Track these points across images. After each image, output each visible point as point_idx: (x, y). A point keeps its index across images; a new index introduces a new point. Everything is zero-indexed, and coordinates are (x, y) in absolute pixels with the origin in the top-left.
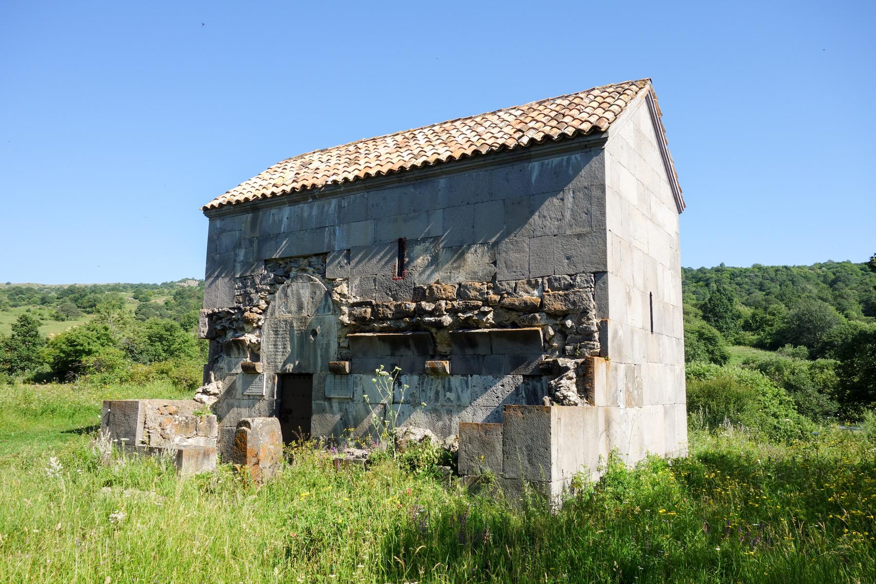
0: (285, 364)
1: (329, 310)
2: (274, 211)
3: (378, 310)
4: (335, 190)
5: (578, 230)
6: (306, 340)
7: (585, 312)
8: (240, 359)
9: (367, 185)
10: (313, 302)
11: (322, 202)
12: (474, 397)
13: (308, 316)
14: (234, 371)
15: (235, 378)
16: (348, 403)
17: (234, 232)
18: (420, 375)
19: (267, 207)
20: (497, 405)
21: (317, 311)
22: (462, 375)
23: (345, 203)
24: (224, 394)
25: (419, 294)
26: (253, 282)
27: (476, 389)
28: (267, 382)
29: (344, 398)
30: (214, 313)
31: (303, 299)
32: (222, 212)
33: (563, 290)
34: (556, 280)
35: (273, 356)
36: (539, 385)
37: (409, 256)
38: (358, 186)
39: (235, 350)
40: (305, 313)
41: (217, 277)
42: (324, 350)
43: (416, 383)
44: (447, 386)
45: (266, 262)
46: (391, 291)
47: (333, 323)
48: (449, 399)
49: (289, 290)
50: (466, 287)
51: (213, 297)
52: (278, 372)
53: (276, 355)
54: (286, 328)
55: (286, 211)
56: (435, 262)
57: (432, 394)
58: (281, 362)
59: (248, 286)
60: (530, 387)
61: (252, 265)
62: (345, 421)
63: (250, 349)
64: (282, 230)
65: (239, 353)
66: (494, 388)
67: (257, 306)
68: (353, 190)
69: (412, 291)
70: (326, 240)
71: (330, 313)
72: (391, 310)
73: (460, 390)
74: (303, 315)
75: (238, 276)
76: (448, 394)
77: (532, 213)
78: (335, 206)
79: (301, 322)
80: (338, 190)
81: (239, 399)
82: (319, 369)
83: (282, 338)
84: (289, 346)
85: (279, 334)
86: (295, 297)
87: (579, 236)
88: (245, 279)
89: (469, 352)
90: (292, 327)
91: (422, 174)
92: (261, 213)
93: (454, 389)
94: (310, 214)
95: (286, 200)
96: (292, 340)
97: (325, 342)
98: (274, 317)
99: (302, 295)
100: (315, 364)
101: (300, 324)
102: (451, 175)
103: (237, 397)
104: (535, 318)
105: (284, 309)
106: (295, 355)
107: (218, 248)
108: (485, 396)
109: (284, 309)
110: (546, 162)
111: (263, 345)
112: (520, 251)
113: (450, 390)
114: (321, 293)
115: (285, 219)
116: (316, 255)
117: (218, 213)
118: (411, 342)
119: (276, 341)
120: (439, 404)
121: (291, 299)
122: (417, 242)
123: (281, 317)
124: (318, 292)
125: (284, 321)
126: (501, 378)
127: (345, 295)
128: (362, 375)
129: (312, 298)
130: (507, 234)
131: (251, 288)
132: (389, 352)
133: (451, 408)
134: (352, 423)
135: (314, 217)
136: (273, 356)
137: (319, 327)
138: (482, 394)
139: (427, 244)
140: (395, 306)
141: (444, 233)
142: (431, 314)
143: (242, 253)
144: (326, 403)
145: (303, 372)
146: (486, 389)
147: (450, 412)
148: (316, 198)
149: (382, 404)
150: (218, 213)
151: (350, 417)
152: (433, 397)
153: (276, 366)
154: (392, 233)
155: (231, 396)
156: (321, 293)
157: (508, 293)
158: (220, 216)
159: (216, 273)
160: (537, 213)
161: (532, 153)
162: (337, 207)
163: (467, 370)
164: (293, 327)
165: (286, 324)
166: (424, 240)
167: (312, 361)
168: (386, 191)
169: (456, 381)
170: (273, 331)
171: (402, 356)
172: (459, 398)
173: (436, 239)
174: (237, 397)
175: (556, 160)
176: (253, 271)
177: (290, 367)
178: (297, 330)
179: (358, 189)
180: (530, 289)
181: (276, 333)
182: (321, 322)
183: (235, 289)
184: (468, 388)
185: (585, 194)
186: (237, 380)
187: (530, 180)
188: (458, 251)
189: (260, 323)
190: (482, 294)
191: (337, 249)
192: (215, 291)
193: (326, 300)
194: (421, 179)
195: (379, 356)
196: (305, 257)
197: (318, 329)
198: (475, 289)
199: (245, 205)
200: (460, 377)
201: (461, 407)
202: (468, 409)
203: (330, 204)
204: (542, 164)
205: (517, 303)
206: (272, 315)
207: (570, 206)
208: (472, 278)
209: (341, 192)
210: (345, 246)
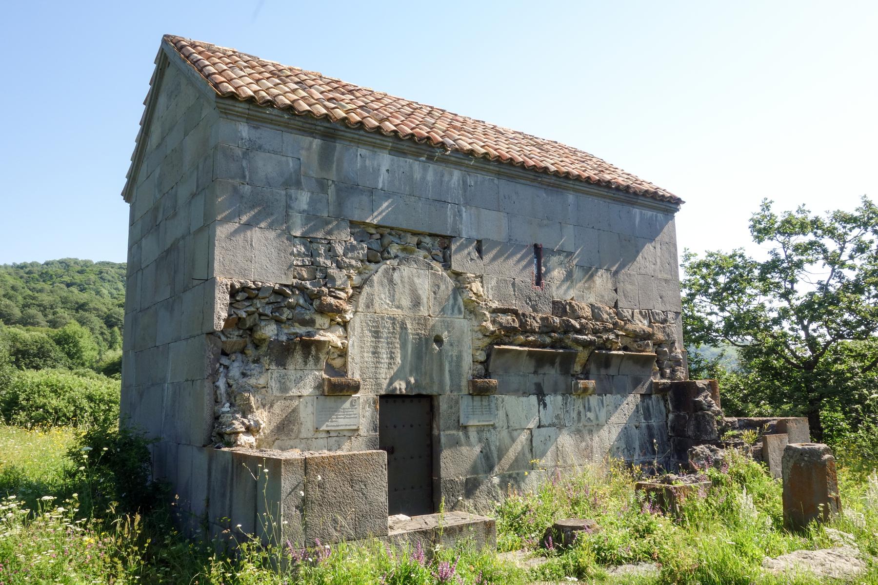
0: (391, 383)
1: (460, 312)
2: (362, 151)
3: (526, 321)
4: (463, 161)
5: (665, 276)
6: (427, 349)
7: (673, 343)
8: (306, 372)
9: (502, 170)
10: (435, 298)
11: (441, 168)
12: (609, 416)
13: (429, 316)
14: (294, 392)
15: (296, 403)
16: (489, 430)
17: (284, 159)
18: (563, 395)
19: (351, 141)
20: (625, 422)
21: (443, 310)
22: (599, 395)
23: (471, 181)
24: (272, 431)
25: (559, 308)
26: (330, 249)
27: (610, 408)
29: (484, 425)
30: (244, 288)
31: (420, 292)
32: (259, 114)
33: (661, 323)
34: (657, 314)
36: (650, 402)
37: (545, 266)
38: (491, 167)
39: (298, 357)
40: (424, 311)
41: (248, 225)
42: (454, 364)
43: (561, 403)
44: (587, 405)
45: (353, 224)
46: (530, 300)
47: (466, 330)
48: (589, 419)
49: (396, 276)
50: (599, 309)
51: (239, 259)
52: (383, 392)
53: (377, 367)
54: (394, 329)
55: (385, 160)
56: (569, 276)
57: (574, 415)
58: (385, 379)
59: (319, 255)
60: (645, 404)
61: (327, 223)
62: (487, 454)
64: (380, 186)
65: (306, 363)
66: (622, 406)
67: (342, 290)
68: (482, 169)
69: (551, 305)
70: (450, 220)
71: (462, 316)
72: (537, 322)
73: (597, 409)
74: (420, 314)
75: (298, 233)
76: (589, 414)
77: (638, 252)
78: (458, 181)
79: (418, 324)
80: (466, 162)
81: (308, 439)
82: (448, 388)
83: (388, 343)
84: (399, 355)
85: (381, 337)
86: (407, 286)
87: (666, 281)
88: (311, 242)
89: (603, 372)
90: (403, 327)
91: (558, 183)
92: (339, 146)
93: (593, 408)
94: (424, 178)
95: (390, 144)
96: (403, 346)
97: (455, 353)
98: (371, 310)
99: (419, 286)
102: (578, 194)
103: (303, 435)
104: (648, 345)
105: (388, 302)
106: (407, 369)
107: (247, 173)
108: (616, 414)
109: (388, 302)
110: (643, 211)
111: (353, 352)
112: (632, 283)
113: (590, 410)
114: (447, 288)
116: (430, 235)
117: (251, 112)
118: (558, 360)
119: (376, 347)
120: (581, 424)
121: (399, 288)
122: (553, 253)
123: (384, 312)
124: (443, 287)
125: (390, 318)
126: (626, 397)
127: (481, 296)
128: (503, 396)
129: (435, 293)
130: (622, 266)
131: (326, 258)
132: (532, 369)
133: (592, 428)
134: (495, 455)
135: (430, 184)
137: (446, 333)
138: (614, 412)
139: (562, 258)
140: (541, 319)
141: (576, 250)
142: (579, 332)
143: (303, 200)
144: (461, 433)
145: (424, 393)
146: (616, 408)
147: (591, 432)
148: (432, 160)
149: (529, 429)
150: (251, 112)
151: (493, 448)
152: (576, 419)
153: (378, 385)
154: (528, 235)
155: (288, 435)
156: (447, 288)
157: (629, 320)
158: (247, 119)
159: (245, 219)
160: (641, 254)
161: (639, 201)
162: (461, 182)
163: (602, 391)
164: (406, 328)
165: (394, 323)
166: (560, 252)
167: (436, 378)
168: (518, 185)
169: (594, 400)
170: (371, 331)
171: (544, 374)
172: (597, 418)
173: (570, 254)
174: (303, 435)
175: (649, 213)
176: (330, 233)
177: (400, 386)
178: (413, 334)
179: (488, 171)
180: (642, 319)
181: (376, 334)
182: (449, 327)
183: (292, 254)
184: (603, 406)
185: (667, 249)
186: (302, 407)
187: (634, 224)
188: (589, 272)
190: (611, 318)
191: (464, 235)
192: (244, 248)
193: (455, 299)
194: (552, 186)
195: (521, 373)
196: (414, 234)
197: (445, 336)
198: (606, 312)
199: (315, 122)
200: (596, 396)
201: (599, 426)
202: (606, 428)
203: (451, 175)
204: (641, 213)
205: (638, 330)
206: (368, 307)
207: (659, 254)
208: (600, 301)
209: (468, 166)
210: (474, 235)
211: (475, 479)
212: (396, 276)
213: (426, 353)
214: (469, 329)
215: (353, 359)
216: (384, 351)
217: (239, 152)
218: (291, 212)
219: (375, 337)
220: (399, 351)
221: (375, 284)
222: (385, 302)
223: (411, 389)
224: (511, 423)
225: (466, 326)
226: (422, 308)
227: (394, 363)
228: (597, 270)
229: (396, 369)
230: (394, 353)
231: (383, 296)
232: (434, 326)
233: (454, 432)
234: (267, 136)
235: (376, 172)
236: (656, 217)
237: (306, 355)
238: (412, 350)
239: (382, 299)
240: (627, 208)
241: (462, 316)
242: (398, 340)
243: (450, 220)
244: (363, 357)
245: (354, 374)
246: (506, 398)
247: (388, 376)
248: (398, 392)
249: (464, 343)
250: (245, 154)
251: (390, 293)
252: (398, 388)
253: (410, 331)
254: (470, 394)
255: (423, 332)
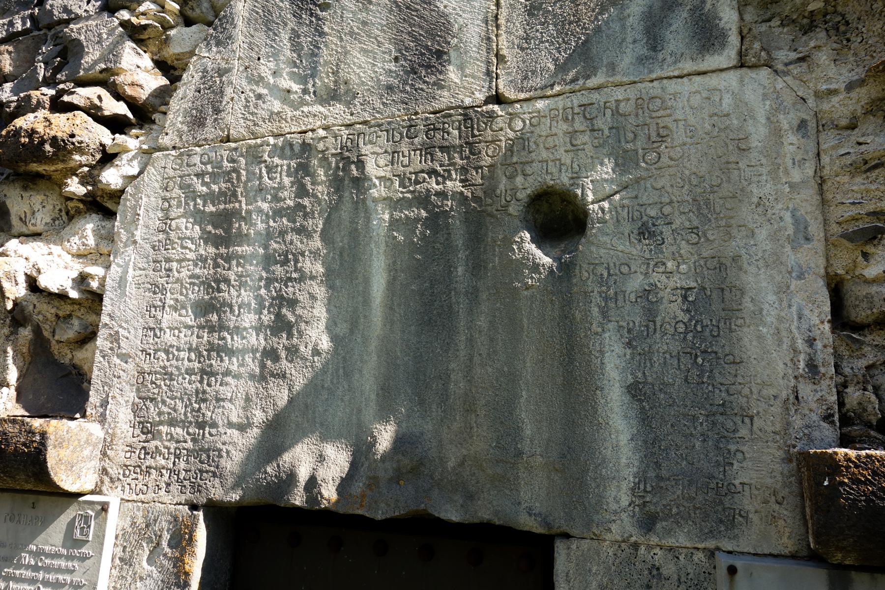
6: (477, 267)
13: (498, 99)
28: (126, 561)
35: (189, 385)
47: (758, 133)
52: (217, 492)
53: (207, 373)
54: (302, 191)
58: (242, 428)
63: (26, 333)
74: (445, 99)
79: (428, 150)
83: (268, 261)
84: (320, 312)
98: (210, 132)
101: (418, 162)
105: (286, 83)
109: (286, 83)
119: (215, 283)
125: (285, 150)
136: (189, 385)
137: (606, 170)
164: (360, 182)
165: (304, 169)
170: (199, 217)
178: (394, 204)
189: (111, 177)
206: (198, 122)
213: (473, 295)
214: (786, 122)
215: (115, 338)
216: (246, 296)
219: (217, 241)
220: (320, 291)
221: (240, 31)
222: (274, 89)
223: (373, 482)
225: (761, 111)
226: (453, 74)
227: (293, 352)
229: (300, 378)
230: (293, 303)
231: (265, 68)
232: (521, 142)
238: (391, 283)
239: (259, 80)
241: (727, 56)
242: (317, 243)
244: (154, 330)
247: (259, 417)
248: (298, 499)
249: (747, 214)
251: (296, 47)
252: (303, 474)
253: (378, 191)
254: (815, 558)
255: (454, 185)
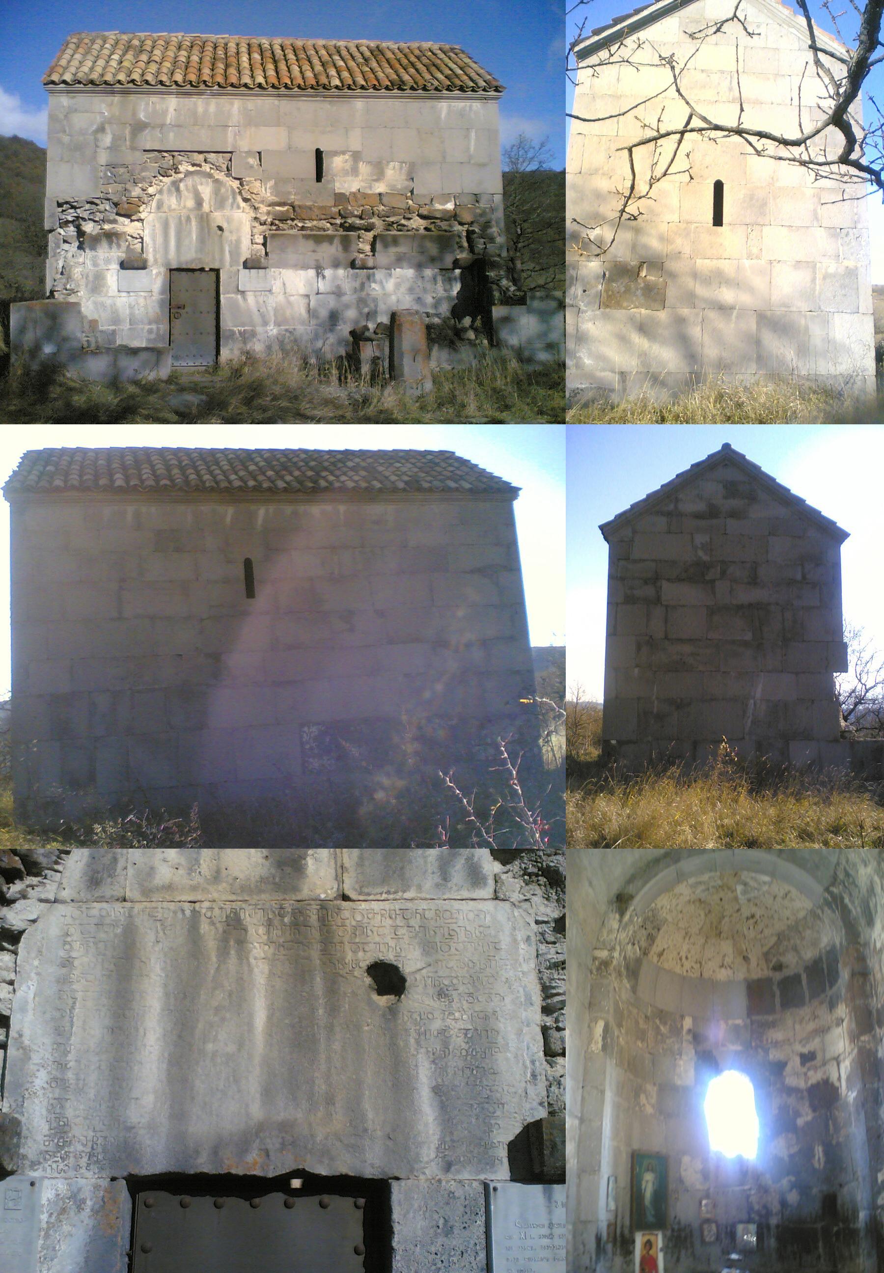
64: (168, 121)
65: (111, 248)
94: (206, 111)
97: (234, 238)
100: (222, 260)
115: (171, 110)
121: (185, 193)
122: (336, 153)
144: (239, 297)
151: (269, 308)
167: (217, 257)
168: (300, 103)
187: (439, 117)
196: (200, 152)
204: (450, 106)
211: (252, 330)
212: (182, 185)
217: (61, 116)
218: (98, 150)
224: (288, 290)
228: (388, 162)
233: (233, 295)
234: (81, 100)
235: (165, 112)
236: (471, 107)
237: (110, 243)
240: (429, 103)
243: (230, 139)
245: (150, 256)
246: (283, 271)
250: (66, 116)
